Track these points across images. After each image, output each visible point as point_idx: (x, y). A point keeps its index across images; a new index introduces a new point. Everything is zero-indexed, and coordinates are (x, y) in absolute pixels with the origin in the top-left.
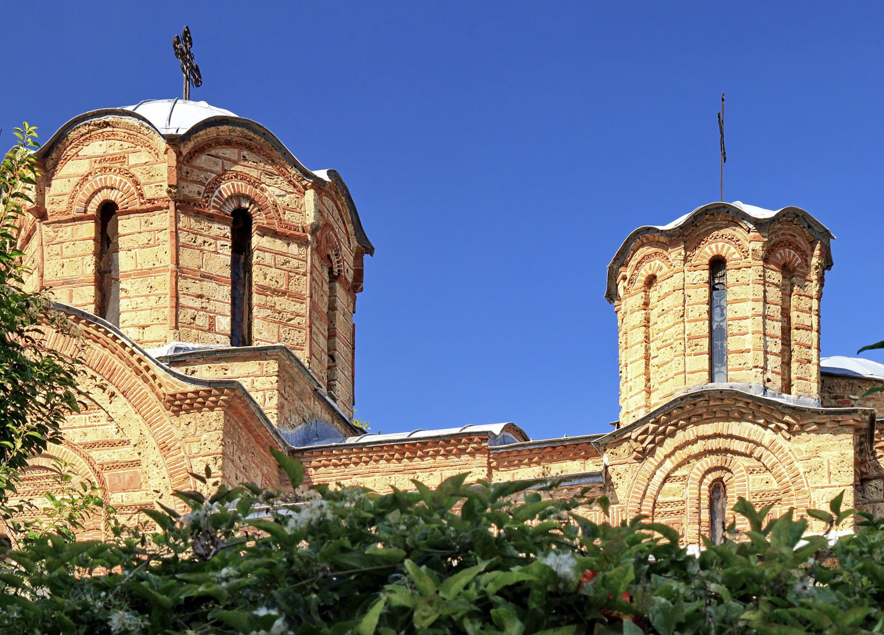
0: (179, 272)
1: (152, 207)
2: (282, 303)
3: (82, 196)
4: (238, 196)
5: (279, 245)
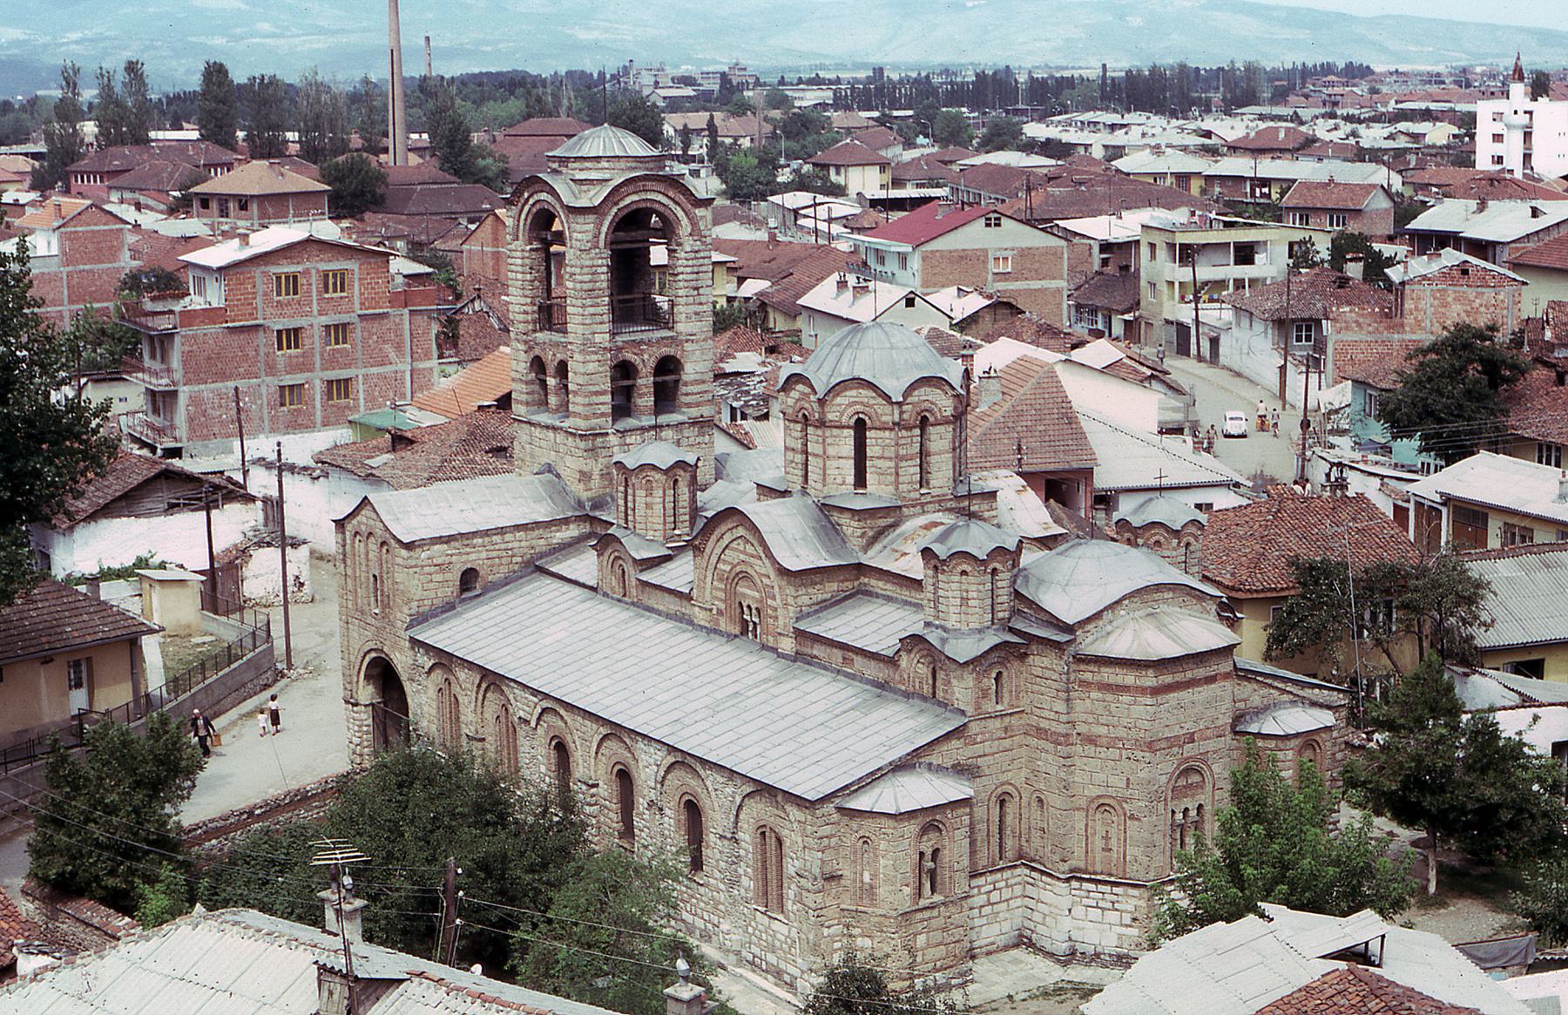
2: (880, 463)
5: (880, 434)
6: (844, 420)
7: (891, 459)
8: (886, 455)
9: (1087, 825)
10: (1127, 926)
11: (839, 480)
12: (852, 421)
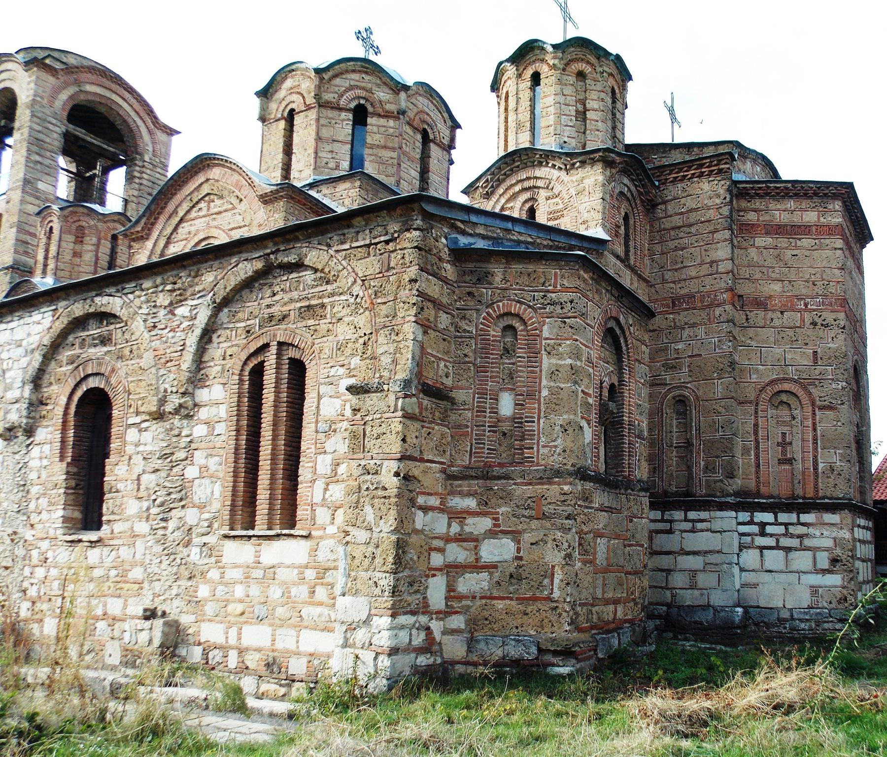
0: (319, 139)
1: (309, 108)
3: (281, 109)
4: (359, 98)
5: (382, 121)
6: (342, 102)
7: (393, 149)
8: (390, 145)
9: (756, 425)
10: (824, 572)
11: (332, 165)
12: (353, 105)
